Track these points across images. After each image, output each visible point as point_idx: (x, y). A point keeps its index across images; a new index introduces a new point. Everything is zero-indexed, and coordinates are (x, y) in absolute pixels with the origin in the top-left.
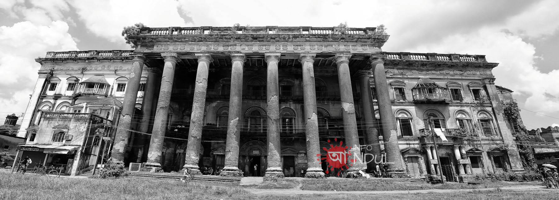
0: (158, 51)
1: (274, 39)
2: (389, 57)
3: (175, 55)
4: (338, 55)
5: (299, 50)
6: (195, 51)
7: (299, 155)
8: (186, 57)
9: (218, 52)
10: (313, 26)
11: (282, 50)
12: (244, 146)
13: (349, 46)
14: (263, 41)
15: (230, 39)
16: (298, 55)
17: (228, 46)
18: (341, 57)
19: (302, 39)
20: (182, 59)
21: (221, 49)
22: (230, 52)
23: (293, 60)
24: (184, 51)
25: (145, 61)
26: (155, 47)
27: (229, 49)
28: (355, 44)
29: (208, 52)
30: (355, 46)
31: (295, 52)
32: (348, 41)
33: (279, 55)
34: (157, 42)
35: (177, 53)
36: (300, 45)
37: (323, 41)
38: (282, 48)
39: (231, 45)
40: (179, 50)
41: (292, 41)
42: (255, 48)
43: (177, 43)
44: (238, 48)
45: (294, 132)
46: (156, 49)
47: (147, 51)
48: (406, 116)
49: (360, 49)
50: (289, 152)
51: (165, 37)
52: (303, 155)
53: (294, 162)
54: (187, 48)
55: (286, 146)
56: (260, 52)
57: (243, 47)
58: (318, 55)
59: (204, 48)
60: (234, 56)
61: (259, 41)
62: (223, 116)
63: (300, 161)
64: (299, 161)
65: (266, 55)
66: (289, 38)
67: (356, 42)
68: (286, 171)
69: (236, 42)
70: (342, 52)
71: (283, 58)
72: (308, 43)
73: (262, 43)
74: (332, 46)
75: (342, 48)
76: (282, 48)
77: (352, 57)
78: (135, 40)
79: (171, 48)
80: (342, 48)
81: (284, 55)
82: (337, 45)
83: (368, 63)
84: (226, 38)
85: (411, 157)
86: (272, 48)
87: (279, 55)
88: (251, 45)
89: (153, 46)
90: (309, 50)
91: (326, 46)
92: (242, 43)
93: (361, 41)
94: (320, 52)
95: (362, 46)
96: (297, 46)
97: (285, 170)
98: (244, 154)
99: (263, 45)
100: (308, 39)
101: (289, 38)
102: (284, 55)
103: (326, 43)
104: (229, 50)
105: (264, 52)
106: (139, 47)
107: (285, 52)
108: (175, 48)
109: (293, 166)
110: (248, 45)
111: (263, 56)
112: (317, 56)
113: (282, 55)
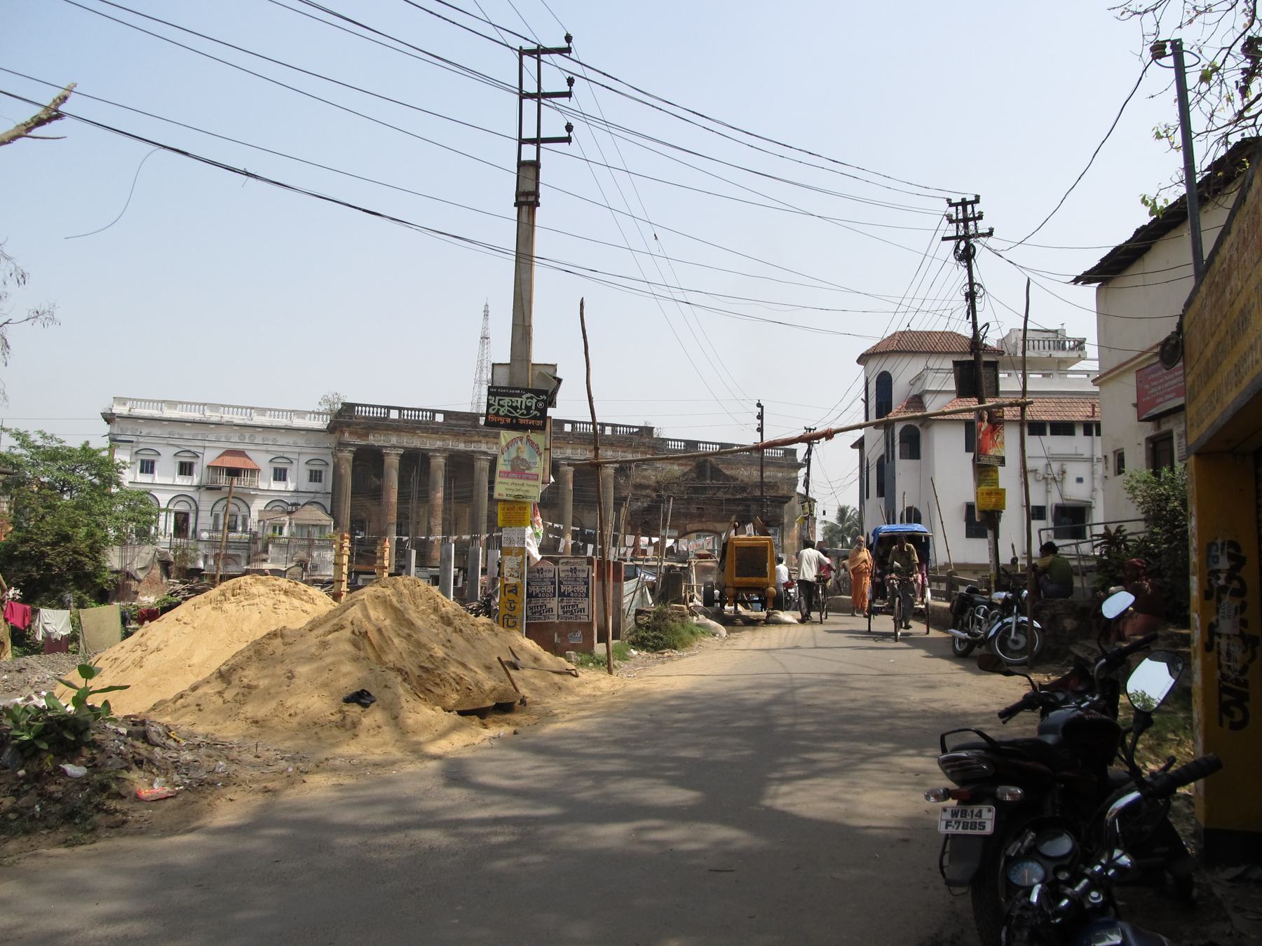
0: (376, 444)
6: (428, 446)
17: (471, 442)
21: (461, 446)
24: (412, 446)
26: (371, 437)
27: (472, 447)
29: (445, 450)
44: (484, 447)
46: (374, 440)
54: (416, 442)
59: (439, 444)
79: (394, 440)
89: (367, 435)
106: (347, 435)
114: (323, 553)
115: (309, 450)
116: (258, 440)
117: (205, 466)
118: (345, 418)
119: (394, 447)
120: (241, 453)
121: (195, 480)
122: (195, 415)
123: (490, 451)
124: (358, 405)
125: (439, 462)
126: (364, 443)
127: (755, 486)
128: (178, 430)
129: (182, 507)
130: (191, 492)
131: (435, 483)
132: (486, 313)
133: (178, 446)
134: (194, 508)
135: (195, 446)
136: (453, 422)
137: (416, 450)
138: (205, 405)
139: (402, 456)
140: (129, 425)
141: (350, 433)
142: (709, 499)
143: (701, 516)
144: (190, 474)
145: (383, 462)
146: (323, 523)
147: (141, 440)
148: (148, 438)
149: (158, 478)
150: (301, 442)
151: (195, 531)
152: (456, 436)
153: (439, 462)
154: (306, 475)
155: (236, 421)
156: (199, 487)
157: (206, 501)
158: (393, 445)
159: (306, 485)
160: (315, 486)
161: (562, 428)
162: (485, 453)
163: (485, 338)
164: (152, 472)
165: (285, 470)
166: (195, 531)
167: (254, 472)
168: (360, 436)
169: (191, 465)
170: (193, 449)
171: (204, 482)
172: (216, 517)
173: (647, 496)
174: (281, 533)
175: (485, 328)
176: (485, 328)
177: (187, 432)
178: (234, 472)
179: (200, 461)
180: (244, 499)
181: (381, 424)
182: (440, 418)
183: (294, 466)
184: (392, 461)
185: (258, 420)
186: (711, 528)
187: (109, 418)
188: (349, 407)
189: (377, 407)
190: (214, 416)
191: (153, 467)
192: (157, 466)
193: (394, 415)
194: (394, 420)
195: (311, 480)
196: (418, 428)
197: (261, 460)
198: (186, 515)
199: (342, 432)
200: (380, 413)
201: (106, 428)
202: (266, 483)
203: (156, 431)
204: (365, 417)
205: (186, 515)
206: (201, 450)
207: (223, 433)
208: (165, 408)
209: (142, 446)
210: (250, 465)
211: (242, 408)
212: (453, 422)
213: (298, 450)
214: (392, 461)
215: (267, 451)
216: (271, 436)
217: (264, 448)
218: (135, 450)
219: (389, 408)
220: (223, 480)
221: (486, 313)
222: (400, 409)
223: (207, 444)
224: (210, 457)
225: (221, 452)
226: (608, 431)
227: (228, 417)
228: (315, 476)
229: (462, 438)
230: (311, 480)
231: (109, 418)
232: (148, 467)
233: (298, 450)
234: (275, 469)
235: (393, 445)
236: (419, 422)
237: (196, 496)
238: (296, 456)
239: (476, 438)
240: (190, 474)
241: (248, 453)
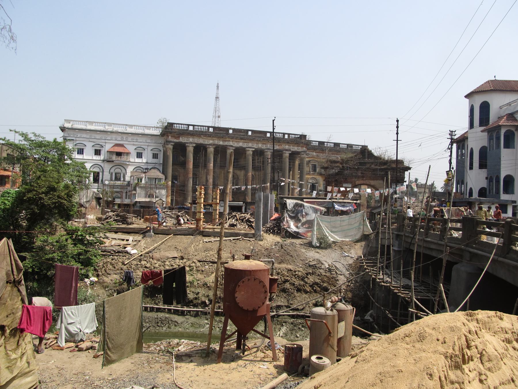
0: (183, 142)
1: (251, 139)
6: (206, 143)
11: (255, 146)
17: (225, 141)
21: (221, 143)
22: (226, 145)
24: (199, 142)
26: (181, 138)
29: (214, 145)
42: (241, 144)
44: (231, 143)
46: (183, 140)
49: (295, 149)
57: (234, 143)
59: (211, 142)
70: (287, 150)
75: (287, 147)
79: (191, 140)
80: (287, 147)
86: (250, 145)
87: (254, 149)
89: (179, 137)
91: (279, 146)
95: (298, 146)
103: (279, 144)
106: (170, 137)
114: (161, 191)
115: (152, 144)
116: (130, 139)
117: (106, 151)
118: (169, 129)
119: (191, 143)
120: (122, 145)
121: (102, 157)
122: (101, 128)
123: (234, 145)
124: (175, 124)
125: (211, 150)
126: (177, 141)
127: (392, 161)
128: (94, 135)
129: (96, 170)
130: (100, 163)
131: (210, 159)
132: (218, 87)
133: (94, 142)
134: (101, 170)
135: (101, 142)
136: (218, 132)
137: (201, 144)
138: (105, 123)
139: (194, 147)
140: (71, 132)
141: (171, 136)
142: (368, 168)
143: (363, 177)
144: (100, 155)
145: (186, 150)
146: (160, 177)
147: (77, 139)
148: (81, 138)
149: (85, 156)
150: (149, 141)
151: (102, 181)
152: (219, 138)
153: (211, 150)
154: (151, 155)
155: (119, 131)
156: (103, 161)
157: (107, 167)
158: (191, 142)
159: (151, 160)
160: (155, 161)
161: (266, 135)
162: (232, 146)
163: (217, 98)
164: (83, 154)
165: (142, 153)
166: (102, 181)
167: (128, 154)
168: (176, 138)
169: (100, 151)
170: (101, 144)
171: (106, 159)
172: (112, 174)
173: (338, 167)
174: (141, 182)
175: (217, 94)
176: (217, 94)
177: (98, 136)
178: (119, 154)
179: (104, 148)
180: (123, 166)
181: (185, 133)
182: (211, 130)
183: (146, 152)
184: (190, 150)
185: (129, 130)
186: (368, 183)
187: (63, 129)
188: (171, 125)
189: (183, 124)
190: (109, 128)
191: (83, 151)
192: (85, 151)
193: (191, 128)
194: (191, 131)
195: (153, 158)
196: (202, 134)
197: (131, 148)
198: (98, 173)
199: (168, 136)
200: (185, 127)
201: (62, 134)
202: (133, 159)
203: (84, 135)
204: (178, 129)
205: (98, 173)
206: (104, 144)
207: (114, 136)
208: (88, 125)
209: (78, 142)
210: (127, 152)
211: (122, 125)
212: (218, 132)
213: (147, 144)
214: (190, 150)
215: (134, 145)
216: (135, 137)
217: (132, 143)
218: (75, 144)
219: (189, 125)
220: (114, 158)
221: (218, 87)
222: (194, 126)
223: (107, 141)
224: (108, 147)
225: (113, 145)
226: (286, 136)
227: (116, 129)
228: (155, 156)
229: (222, 139)
230: (153, 158)
231: (63, 129)
232: (81, 152)
233: (147, 144)
234: (137, 153)
235: (191, 142)
236: (202, 132)
237: (102, 165)
238: (146, 147)
239: (228, 139)
240: (100, 155)
241: (125, 145)
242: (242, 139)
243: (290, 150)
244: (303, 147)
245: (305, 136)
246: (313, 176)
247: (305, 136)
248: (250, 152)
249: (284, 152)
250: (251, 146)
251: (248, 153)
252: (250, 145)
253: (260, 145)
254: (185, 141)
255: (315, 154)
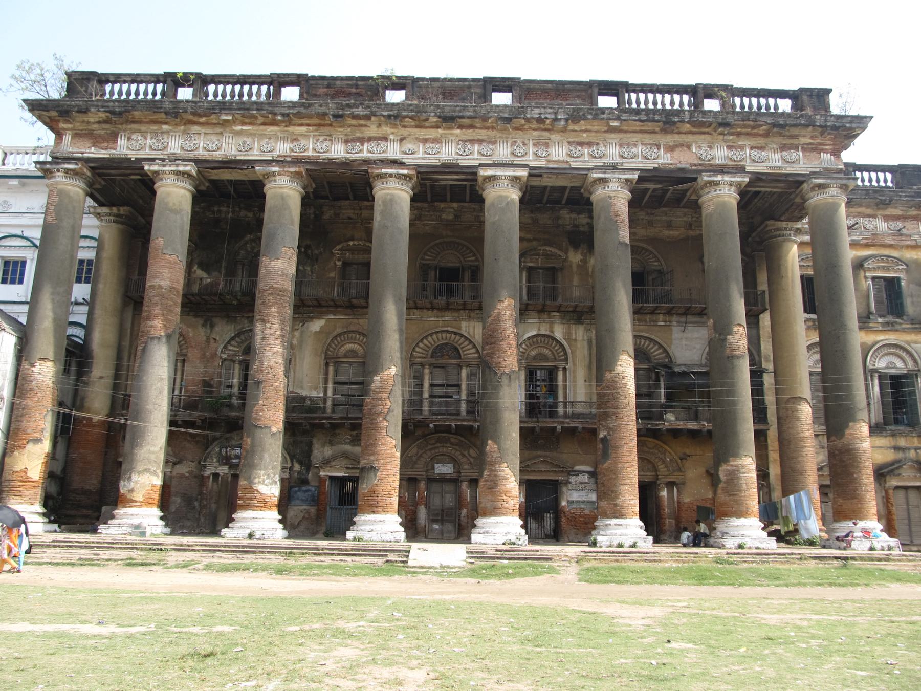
0: (133, 155)
2: (864, 179)
3: (191, 168)
4: (706, 178)
5: (584, 159)
6: (255, 155)
7: (573, 479)
8: (226, 175)
9: (330, 162)
10: (632, 81)
11: (532, 156)
12: (413, 451)
13: (742, 148)
14: (471, 127)
15: (367, 118)
16: (582, 174)
17: (362, 141)
18: (717, 184)
19: (595, 123)
20: (213, 182)
21: (338, 151)
22: (366, 162)
23: (566, 187)
24: (218, 155)
25: (90, 185)
26: (122, 142)
27: (365, 152)
28: (762, 141)
29: (296, 161)
30: (761, 148)
31: (574, 165)
32: (739, 134)
33: (523, 173)
34: (128, 122)
35: (197, 161)
36: (590, 144)
37: (664, 131)
38: (531, 150)
39: (370, 139)
40: (201, 153)
41: (564, 130)
43: (195, 128)
44: (393, 151)
45: (561, 410)
46: (126, 147)
47: (102, 154)
48: (900, 364)
49: (771, 160)
50: (543, 467)
51: (152, 106)
52: (586, 478)
53: (557, 501)
54: (228, 146)
55: (535, 453)
56: (462, 163)
57: (409, 146)
58: (646, 176)
59: (283, 148)
60: (381, 176)
61: (461, 127)
62: (352, 370)
63: (575, 496)
64: (576, 495)
65: (483, 172)
66: (556, 120)
67: (767, 135)
68: (533, 524)
69: (386, 130)
71: (536, 182)
72: (614, 138)
73: (470, 134)
74: (689, 147)
76: (531, 150)
77: (749, 184)
78: (54, 114)
79: (175, 145)
80: (720, 154)
81: (540, 176)
82: (704, 145)
83: (798, 200)
84: (355, 117)
85: (906, 488)
86: (502, 152)
87: (523, 173)
88: (436, 141)
89: (113, 137)
90: (618, 160)
91: (671, 149)
92: (405, 132)
93: (780, 134)
94: (650, 166)
95: (783, 148)
96: (581, 144)
97: (530, 520)
98: (411, 473)
99: (472, 141)
100: (615, 124)
101: (556, 120)
102: (540, 176)
103: (670, 139)
104: (365, 154)
105: (476, 163)
106: (67, 138)
107: (542, 163)
108: (189, 145)
109: (557, 511)
110: (425, 141)
111: (471, 174)
112: (641, 179)
113: (530, 175)
119: (174, 159)
123: (406, 159)
125: (285, 193)
141: (77, 135)
152: (325, 123)
153: (285, 193)
158: (171, 157)
161: (594, 102)
168: (96, 140)
184: (175, 196)
188: (79, 82)
229: (340, 132)
235: (171, 157)
242: (448, 120)
243: (741, 170)
244: (816, 149)
245: (821, 96)
246: (892, 338)
247: (821, 96)
248: (504, 194)
249: (706, 178)
250: (505, 164)
251: (491, 194)
252: (502, 152)
253: (559, 153)
254: (146, 153)
255: (881, 226)
